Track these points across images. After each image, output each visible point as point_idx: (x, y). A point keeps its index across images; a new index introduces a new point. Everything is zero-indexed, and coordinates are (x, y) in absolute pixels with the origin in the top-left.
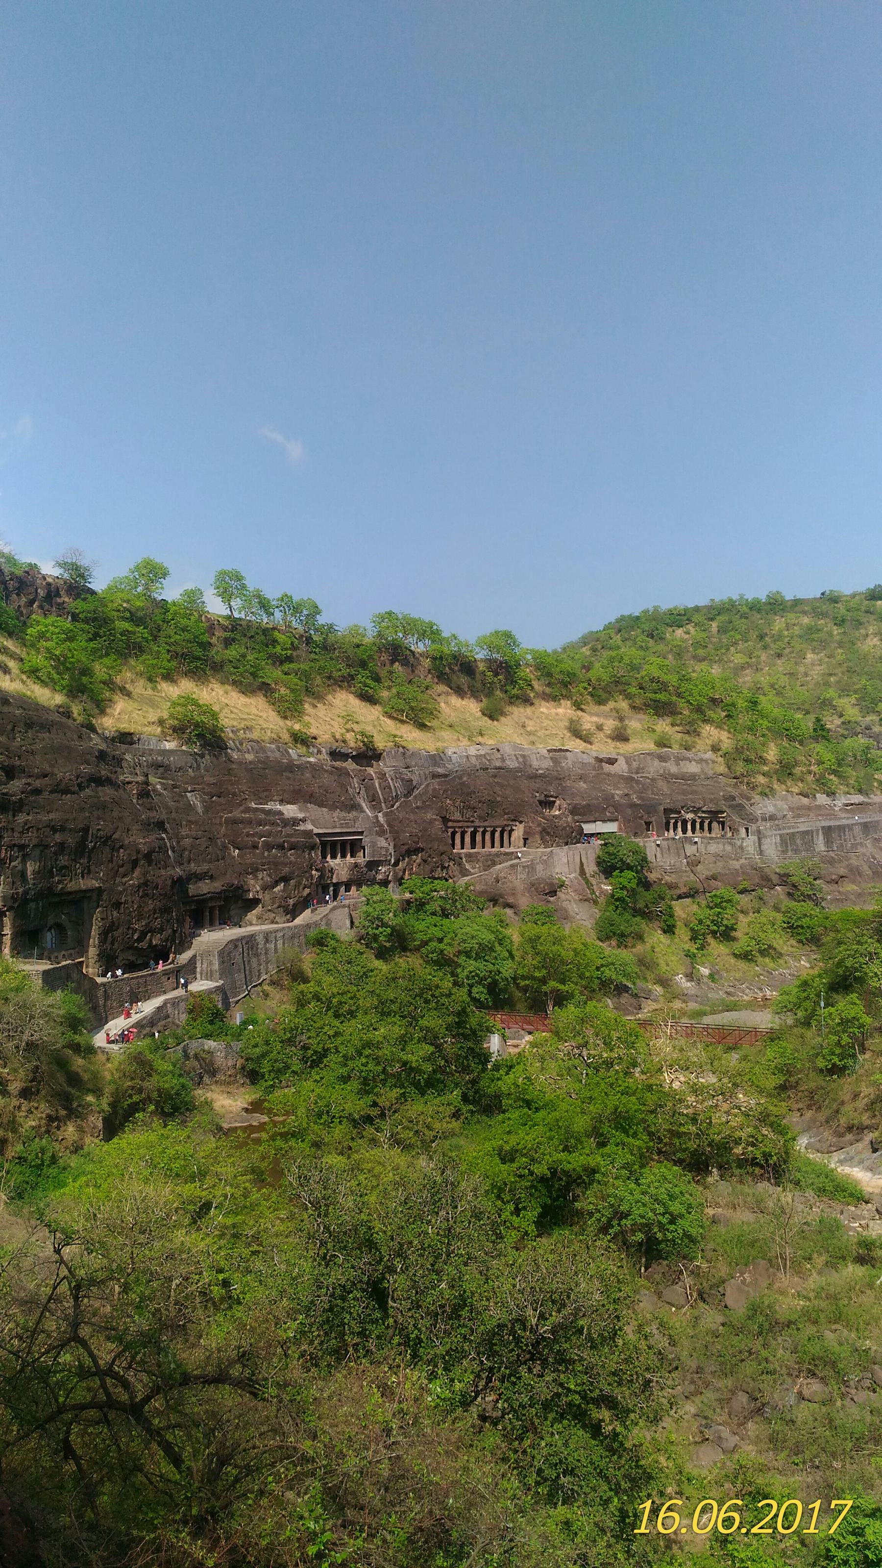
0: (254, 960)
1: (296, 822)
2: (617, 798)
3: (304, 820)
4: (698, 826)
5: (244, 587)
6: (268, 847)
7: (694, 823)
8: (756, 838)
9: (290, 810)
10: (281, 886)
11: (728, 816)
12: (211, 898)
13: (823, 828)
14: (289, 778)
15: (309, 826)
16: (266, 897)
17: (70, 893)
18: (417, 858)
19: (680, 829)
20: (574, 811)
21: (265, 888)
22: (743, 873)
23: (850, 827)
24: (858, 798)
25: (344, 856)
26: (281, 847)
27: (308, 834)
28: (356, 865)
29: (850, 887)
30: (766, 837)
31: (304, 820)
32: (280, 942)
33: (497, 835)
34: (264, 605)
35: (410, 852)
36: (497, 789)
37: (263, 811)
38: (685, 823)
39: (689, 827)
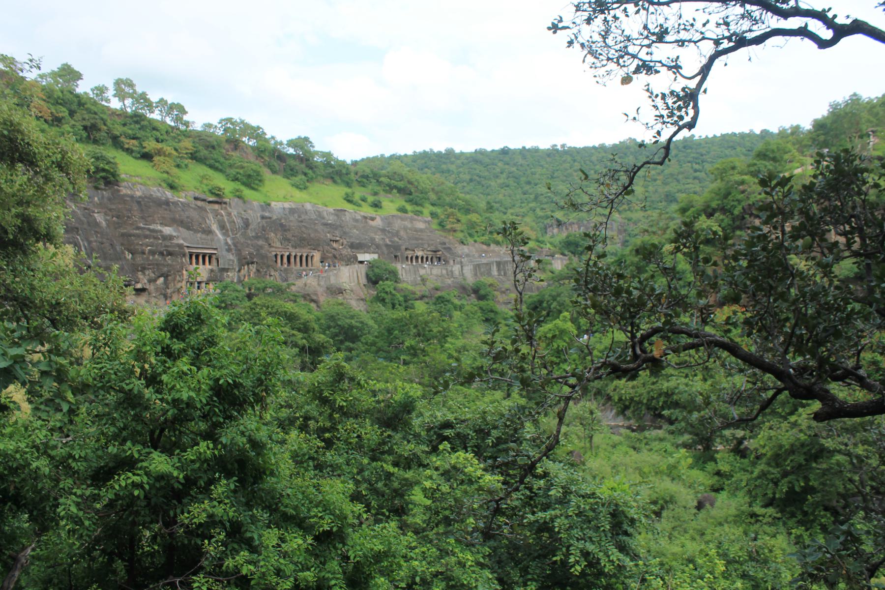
1: (171, 238)
3: (178, 237)
5: (135, 92)
6: (152, 253)
7: (422, 258)
9: (168, 230)
10: (162, 279)
15: (181, 242)
16: (151, 287)
18: (253, 268)
20: (352, 246)
21: (150, 281)
25: (204, 263)
26: (161, 254)
27: (181, 246)
28: (212, 271)
31: (178, 237)
34: (149, 105)
35: (248, 264)
36: (303, 229)
37: (149, 229)
38: (417, 257)
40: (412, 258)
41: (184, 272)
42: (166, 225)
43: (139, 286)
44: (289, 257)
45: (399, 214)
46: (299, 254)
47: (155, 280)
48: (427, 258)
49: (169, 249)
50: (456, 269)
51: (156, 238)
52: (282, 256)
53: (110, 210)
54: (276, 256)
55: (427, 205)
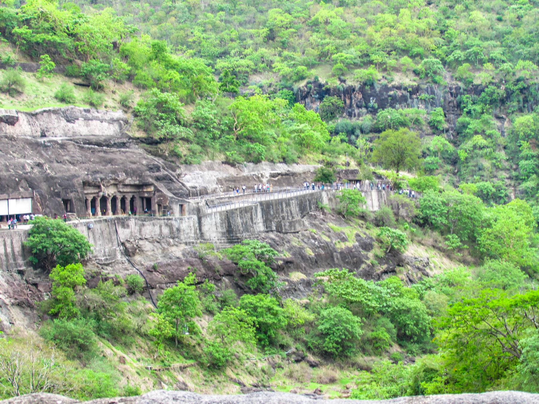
2: (29, 169)
4: (119, 205)
7: (114, 199)
8: (195, 217)
11: (157, 190)
13: (261, 203)
19: (99, 209)
22: (187, 261)
23: (288, 202)
24: (282, 168)
29: (296, 276)
30: (206, 216)
38: (104, 199)
39: (109, 205)
40: (94, 201)
45: (63, 106)
48: (123, 200)
50: (187, 224)
55: (111, 85)
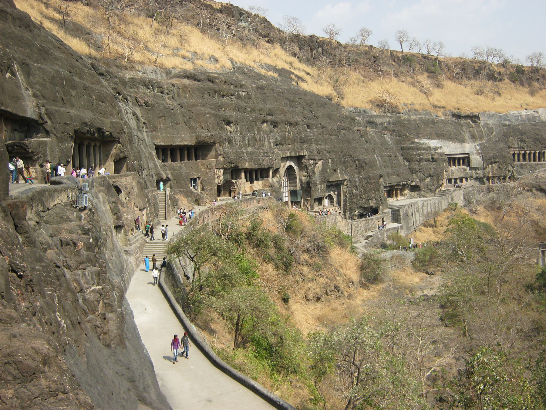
0: (417, 214)
1: (436, 149)
10: (428, 179)
12: (396, 185)
14: (432, 128)
16: (421, 185)
17: (334, 181)
21: (420, 181)
25: (459, 164)
32: (429, 206)
33: (537, 155)
41: (445, 173)
42: (432, 140)
43: (413, 184)
44: (524, 155)
46: (533, 152)
47: (424, 180)
49: (434, 157)
51: (424, 149)
52: (519, 154)
53: (394, 131)
54: (514, 154)
